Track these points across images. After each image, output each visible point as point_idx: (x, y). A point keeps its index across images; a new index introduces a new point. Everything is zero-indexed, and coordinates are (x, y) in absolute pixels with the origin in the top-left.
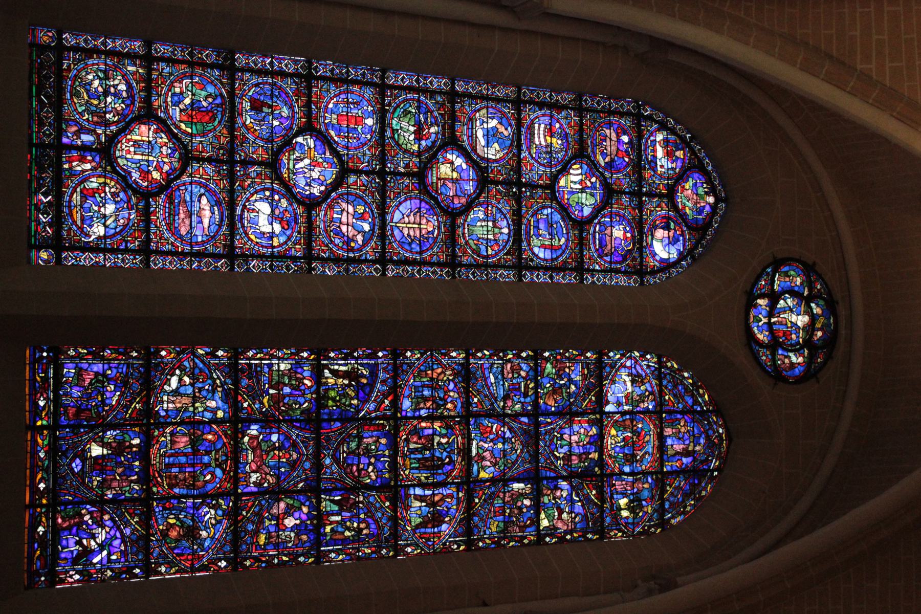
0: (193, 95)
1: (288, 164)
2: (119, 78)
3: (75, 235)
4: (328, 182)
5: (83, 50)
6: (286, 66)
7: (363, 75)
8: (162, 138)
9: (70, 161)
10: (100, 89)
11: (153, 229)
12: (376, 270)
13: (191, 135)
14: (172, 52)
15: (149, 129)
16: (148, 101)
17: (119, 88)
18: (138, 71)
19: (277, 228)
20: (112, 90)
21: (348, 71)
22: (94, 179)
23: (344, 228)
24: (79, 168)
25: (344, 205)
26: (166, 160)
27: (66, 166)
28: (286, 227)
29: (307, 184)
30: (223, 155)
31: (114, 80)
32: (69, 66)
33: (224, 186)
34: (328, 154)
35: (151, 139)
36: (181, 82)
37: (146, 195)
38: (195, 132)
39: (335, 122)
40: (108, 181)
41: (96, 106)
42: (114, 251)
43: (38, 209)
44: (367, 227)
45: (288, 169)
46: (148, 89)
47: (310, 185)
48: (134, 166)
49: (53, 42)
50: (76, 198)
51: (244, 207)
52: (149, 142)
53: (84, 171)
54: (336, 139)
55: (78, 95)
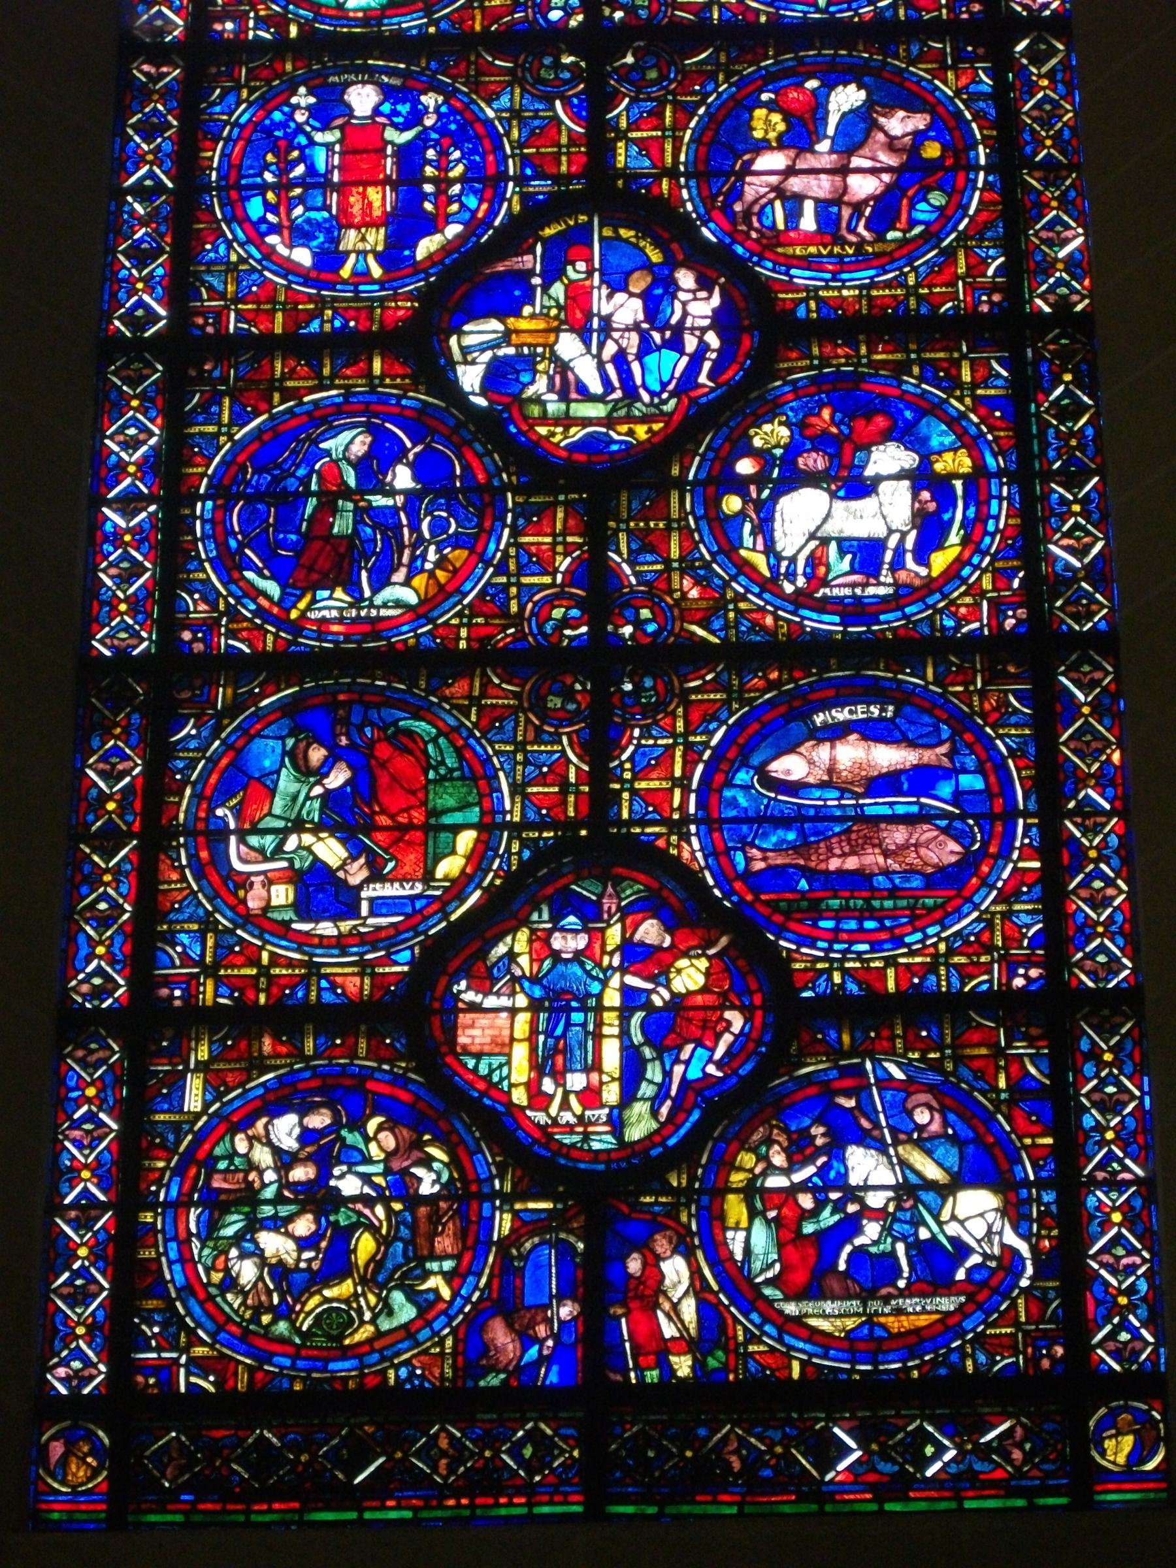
0: (298, 825)
1: (585, 422)
2: (241, 1145)
3: (1010, 1317)
4: (655, 257)
5: (122, 1308)
6: (131, 445)
7: (149, 131)
8: (511, 956)
9: (662, 1351)
10: (304, 1226)
11: (943, 981)
12: (1036, 57)
13: (489, 828)
14: (104, 922)
15: (474, 1008)
16: (342, 1018)
17: (289, 1143)
18: (201, 1067)
19: (888, 458)
20: (300, 1173)
21: (139, 191)
22: (736, 1243)
23: (863, 186)
24: (689, 1310)
25: (754, 188)
26: (614, 935)
27: (683, 1365)
28: (881, 421)
29: (676, 344)
30: (568, 694)
31: (252, 1166)
32: (199, 1366)
33: (715, 686)
34: (527, 261)
35: (521, 1001)
36: (245, 882)
37: (790, 1020)
38: (474, 815)
39: (376, 238)
40: (737, 1178)
41: (384, 1242)
42: (1071, 1147)
43: (900, 1486)
44: (847, 98)
45: (609, 421)
46: (288, 1017)
47: (679, 329)
48: (654, 1073)
49: (91, 1437)
50: (831, 1316)
51: (801, 600)
52: (535, 1006)
53: (698, 1286)
54: (453, 230)
55: (337, 1321)
